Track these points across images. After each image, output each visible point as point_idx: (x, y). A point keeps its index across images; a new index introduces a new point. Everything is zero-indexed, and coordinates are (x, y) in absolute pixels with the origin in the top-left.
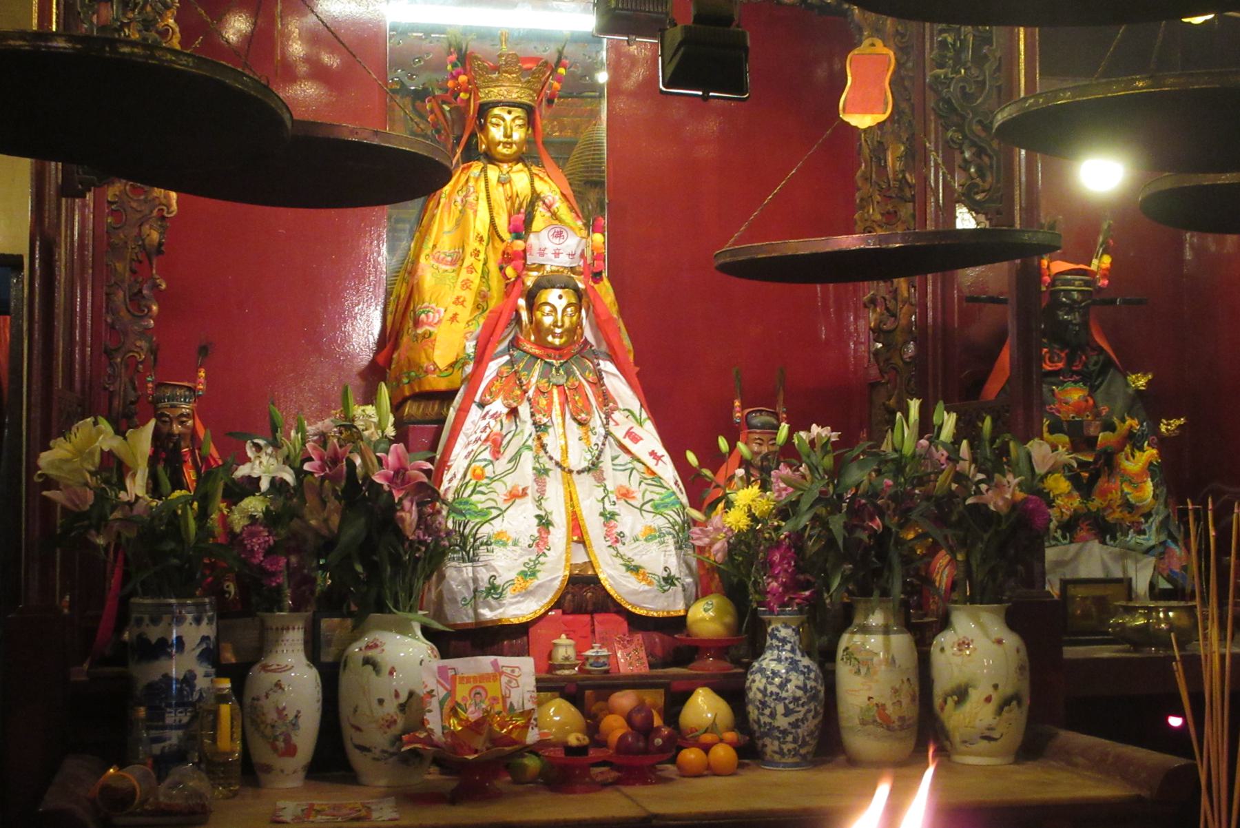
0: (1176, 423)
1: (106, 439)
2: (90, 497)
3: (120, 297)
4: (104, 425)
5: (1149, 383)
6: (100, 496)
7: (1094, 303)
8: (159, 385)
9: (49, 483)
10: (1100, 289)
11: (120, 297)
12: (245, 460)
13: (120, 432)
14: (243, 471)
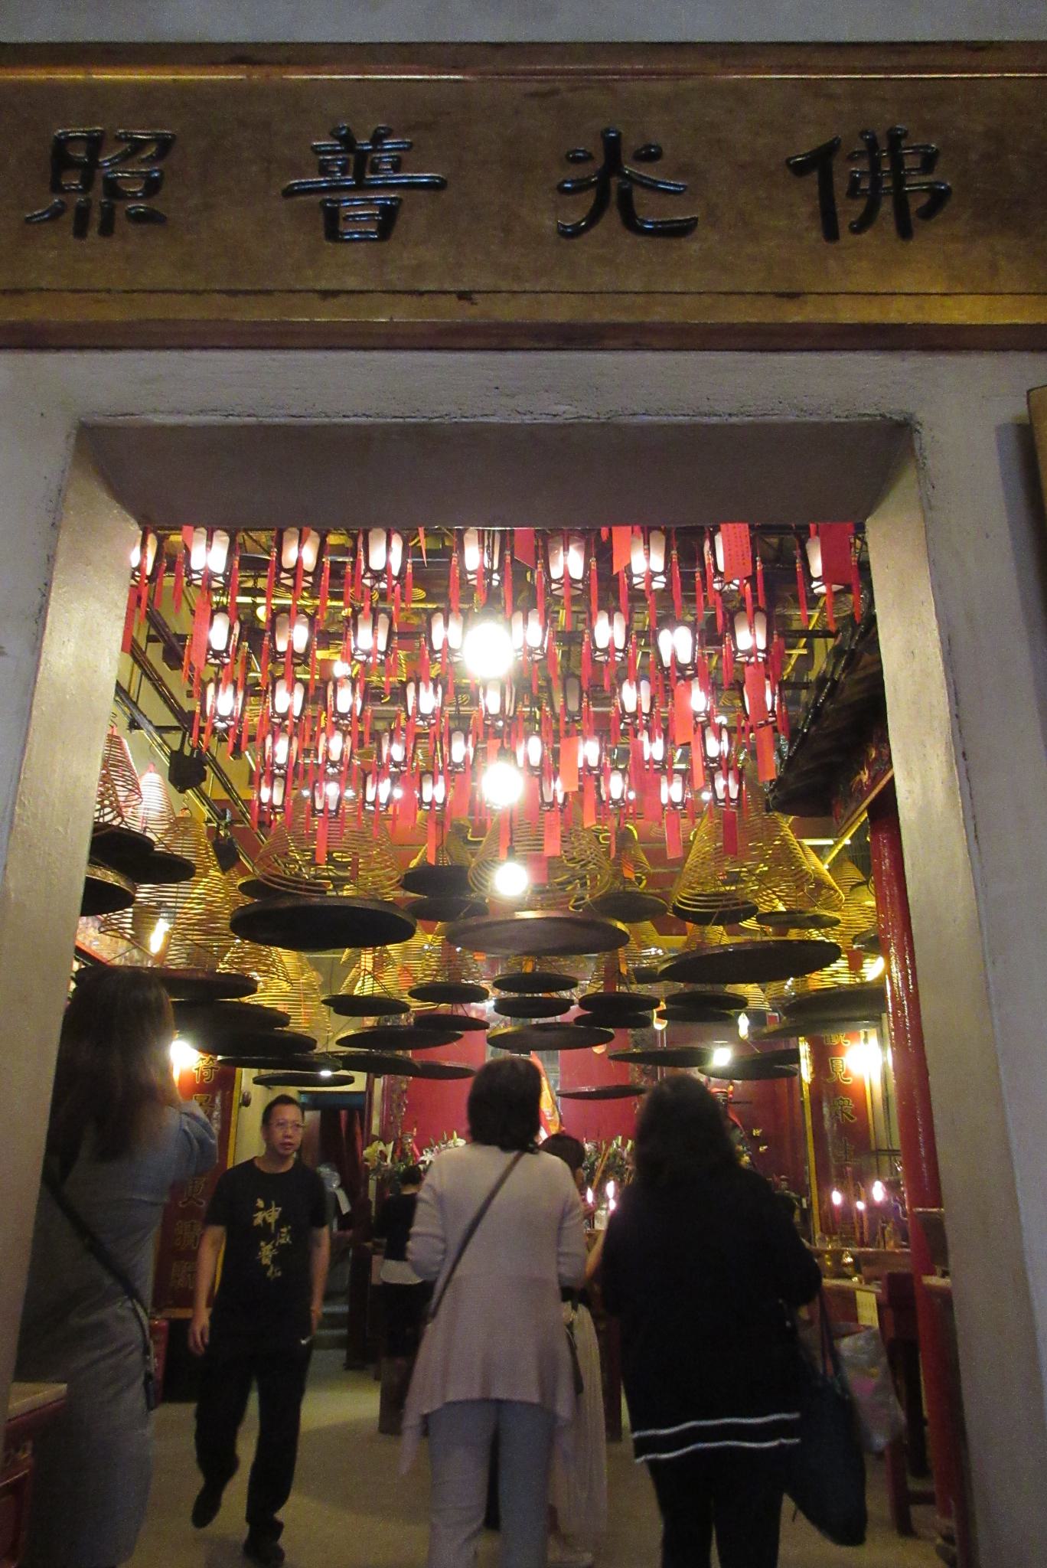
0: (765, 1147)
1: (381, 1147)
2: (376, 1164)
3: (394, 1105)
4: (382, 1143)
5: (761, 1133)
6: (379, 1164)
7: (731, 1103)
8: (403, 1133)
9: (367, 1160)
10: (731, 1099)
11: (394, 1105)
12: (422, 1155)
13: (385, 1145)
14: (422, 1158)
